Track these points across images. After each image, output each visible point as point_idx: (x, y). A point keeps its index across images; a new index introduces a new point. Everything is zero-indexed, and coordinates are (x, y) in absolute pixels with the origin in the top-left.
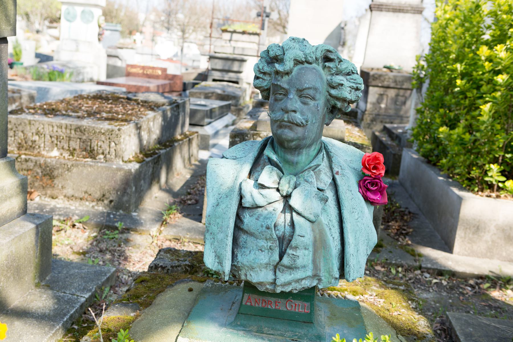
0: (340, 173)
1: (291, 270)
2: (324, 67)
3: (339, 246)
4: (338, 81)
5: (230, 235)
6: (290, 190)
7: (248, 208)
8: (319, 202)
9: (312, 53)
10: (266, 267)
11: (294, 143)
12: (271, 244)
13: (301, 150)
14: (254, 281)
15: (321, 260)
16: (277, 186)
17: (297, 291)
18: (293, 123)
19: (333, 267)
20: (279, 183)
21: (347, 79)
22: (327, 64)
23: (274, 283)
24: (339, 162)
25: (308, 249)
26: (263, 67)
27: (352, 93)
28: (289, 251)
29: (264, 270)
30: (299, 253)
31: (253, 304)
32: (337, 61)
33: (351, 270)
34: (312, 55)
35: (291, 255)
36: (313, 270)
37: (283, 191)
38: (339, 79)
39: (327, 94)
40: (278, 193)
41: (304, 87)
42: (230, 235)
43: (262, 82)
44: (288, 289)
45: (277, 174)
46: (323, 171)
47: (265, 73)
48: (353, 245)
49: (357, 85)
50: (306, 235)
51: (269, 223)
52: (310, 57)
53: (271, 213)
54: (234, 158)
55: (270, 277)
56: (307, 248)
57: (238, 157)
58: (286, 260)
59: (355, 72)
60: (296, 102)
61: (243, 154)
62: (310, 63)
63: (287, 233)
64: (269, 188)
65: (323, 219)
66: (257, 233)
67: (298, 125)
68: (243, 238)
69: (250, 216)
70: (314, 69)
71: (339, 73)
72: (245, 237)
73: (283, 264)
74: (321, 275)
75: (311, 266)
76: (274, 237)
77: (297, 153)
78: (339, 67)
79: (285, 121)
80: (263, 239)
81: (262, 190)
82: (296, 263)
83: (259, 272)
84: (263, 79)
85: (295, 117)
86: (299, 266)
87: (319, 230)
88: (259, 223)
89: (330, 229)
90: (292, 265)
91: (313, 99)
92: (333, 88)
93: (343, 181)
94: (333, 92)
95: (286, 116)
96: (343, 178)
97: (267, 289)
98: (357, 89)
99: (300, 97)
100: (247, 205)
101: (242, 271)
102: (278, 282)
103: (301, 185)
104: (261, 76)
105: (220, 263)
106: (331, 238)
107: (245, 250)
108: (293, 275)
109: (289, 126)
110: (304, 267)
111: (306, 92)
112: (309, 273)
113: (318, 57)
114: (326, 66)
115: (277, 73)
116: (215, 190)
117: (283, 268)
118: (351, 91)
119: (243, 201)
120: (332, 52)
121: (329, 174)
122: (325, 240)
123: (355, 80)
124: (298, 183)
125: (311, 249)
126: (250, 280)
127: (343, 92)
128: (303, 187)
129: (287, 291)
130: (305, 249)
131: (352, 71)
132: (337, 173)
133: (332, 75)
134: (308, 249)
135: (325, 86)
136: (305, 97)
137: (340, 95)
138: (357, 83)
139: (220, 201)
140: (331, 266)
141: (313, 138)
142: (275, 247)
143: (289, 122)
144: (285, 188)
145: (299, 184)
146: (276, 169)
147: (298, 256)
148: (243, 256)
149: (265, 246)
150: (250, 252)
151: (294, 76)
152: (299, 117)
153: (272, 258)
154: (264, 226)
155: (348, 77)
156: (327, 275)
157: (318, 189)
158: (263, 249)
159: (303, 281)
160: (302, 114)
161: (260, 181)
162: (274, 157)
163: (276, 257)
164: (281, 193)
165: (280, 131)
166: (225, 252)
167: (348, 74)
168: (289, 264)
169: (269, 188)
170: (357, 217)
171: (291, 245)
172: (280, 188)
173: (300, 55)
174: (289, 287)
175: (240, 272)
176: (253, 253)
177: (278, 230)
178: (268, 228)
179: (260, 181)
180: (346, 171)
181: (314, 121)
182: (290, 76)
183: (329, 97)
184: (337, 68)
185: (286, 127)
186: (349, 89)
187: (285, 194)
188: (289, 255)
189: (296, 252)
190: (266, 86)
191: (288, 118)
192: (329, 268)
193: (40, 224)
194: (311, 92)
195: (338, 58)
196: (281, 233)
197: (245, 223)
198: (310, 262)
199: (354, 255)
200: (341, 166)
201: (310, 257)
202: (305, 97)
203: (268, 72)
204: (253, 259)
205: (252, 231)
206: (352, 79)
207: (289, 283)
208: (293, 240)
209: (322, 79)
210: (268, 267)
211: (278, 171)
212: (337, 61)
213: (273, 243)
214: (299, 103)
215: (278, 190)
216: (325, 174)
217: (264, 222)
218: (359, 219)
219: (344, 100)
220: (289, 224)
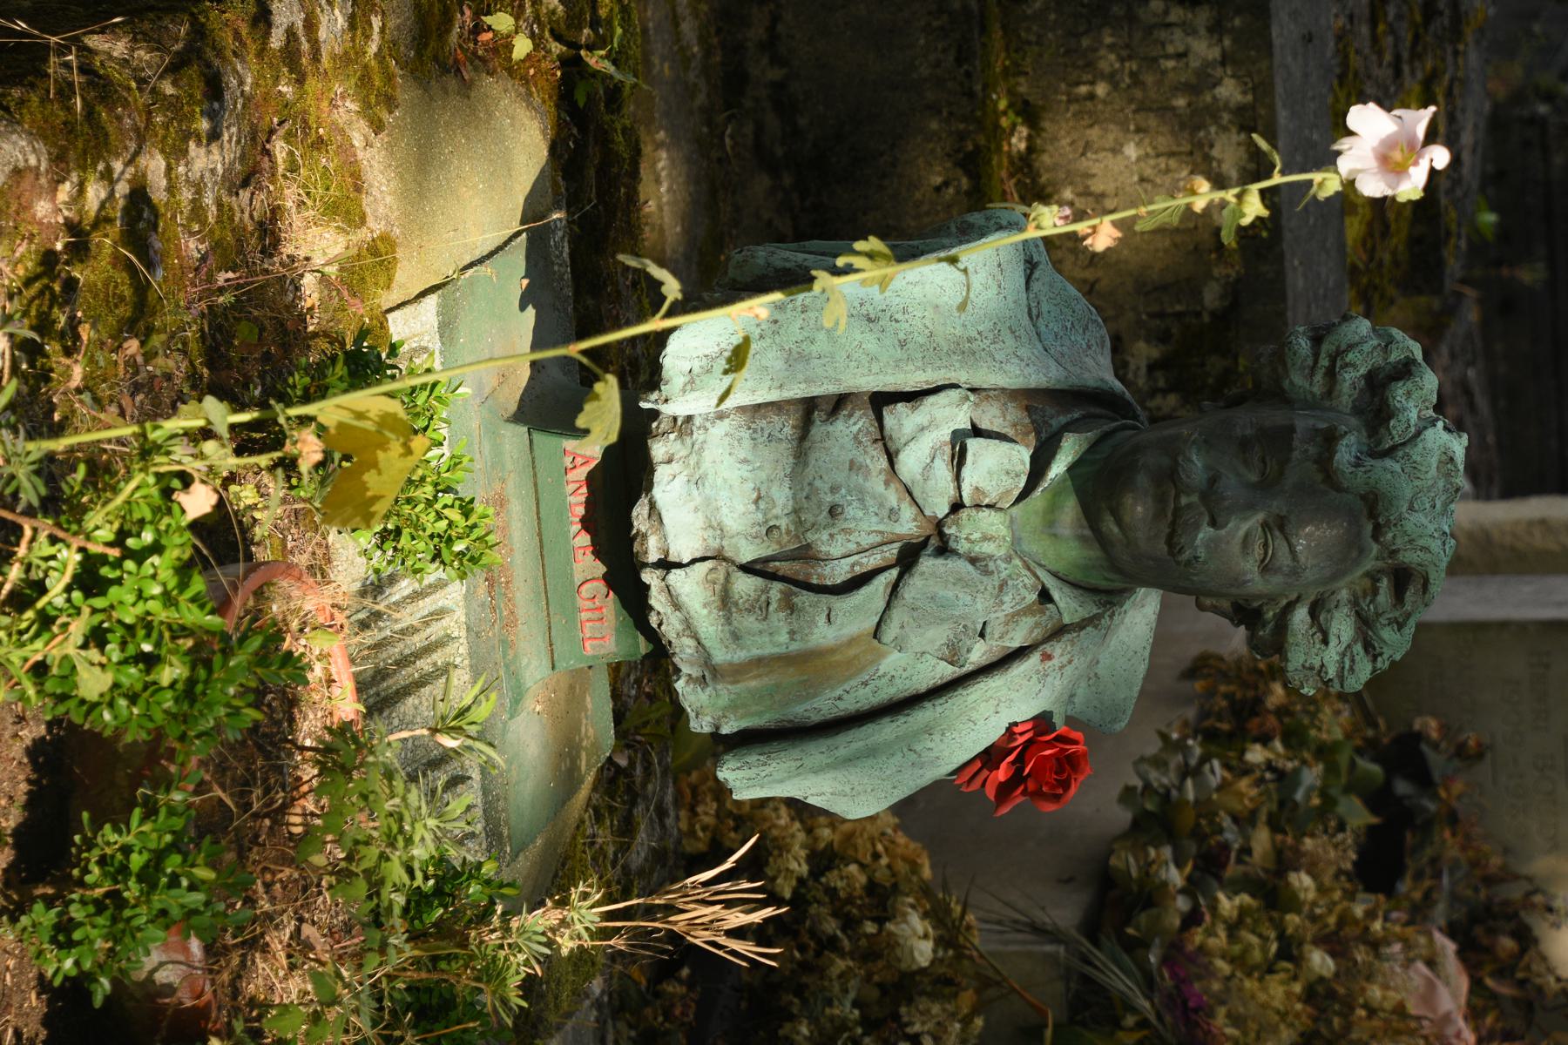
0: (1049, 664)
1: (719, 603)
2: (1373, 577)
3: (816, 718)
4: (1334, 630)
6: (963, 547)
7: (880, 419)
8: (944, 640)
9: (1406, 538)
10: (711, 527)
11: (1116, 530)
12: (783, 528)
14: (657, 492)
15: (766, 680)
16: (967, 500)
17: (655, 626)
18: (1173, 524)
20: (978, 506)
21: (1349, 646)
22: (1384, 584)
23: (666, 565)
25: (792, 639)
26: (1354, 365)
28: (776, 589)
29: (699, 520)
30: (778, 619)
31: (571, 476)
32: (1397, 614)
33: (754, 770)
35: (764, 598)
36: (731, 664)
38: (1343, 627)
39: (1294, 596)
40: (947, 511)
41: (1294, 541)
43: (1302, 368)
44: (657, 600)
45: (1008, 492)
47: (1331, 374)
50: (834, 627)
51: (852, 511)
52: (1394, 537)
53: (881, 505)
54: (1035, 312)
55: (682, 549)
56: (797, 637)
57: (1041, 323)
61: (1051, 337)
63: (828, 569)
64: (958, 478)
66: (810, 471)
69: (856, 437)
71: (1365, 624)
72: (788, 430)
73: (733, 579)
77: (1087, 532)
78: (1383, 621)
79: (1177, 497)
80: (794, 498)
81: (947, 457)
83: (692, 505)
84: (1313, 368)
88: (840, 477)
89: (865, 684)
90: (736, 604)
92: (1313, 613)
93: (1025, 682)
94: (1301, 616)
95: (1195, 498)
97: (645, 536)
100: (889, 420)
101: (678, 445)
102: (675, 576)
103: (985, 579)
104: (1324, 362)
105: (692, 382)
107: (747, 443)
108: (705, 612)
113: (1400, 556)
114: (1378, 581)
115: (1330, 439)
116: (917, 291)
119: (900, 407)
123: (1352, 669)
124: (991, 566)
125: (794, 647)
126: (658, 477)
129: (652, 602)
130: (792, 633)
131: (1381, 654)
134: (792, 639)
136: (1266, 545)
137: (1291, 640)
139: (884, 322)
142: (779, 543)
143: (1177, 511)
144: (966, 533)
146: (1022, 485)
147: (765, 619)
149: (775, 511)
150: (745, 461)
154: (837, 498)
155: (1358, 648)
158: (762, 505)
161: (973, 444)
162: (1058, 468)
163: (747, 553)
164: (949, 520)
165: (1142, 480)
167: (1368, 646)
168: (737, 597)
169: (958, 478)
171: (796, 594)
172: (964, 514)
175: (672, 436)
176: (746, 474)
178: (834, 511)
179: (973, 444)
182: (1322, 486)
183: (1284, 602)
184: (1378, 615)
185: (1161, 500)
186: (1317, 664)
187: (947, 531)
188: (765, 591)
190: (1292, 383)
191: (1189, 506)
195: (1408, 616)
196: (823, 549)
197: (831, 428)
198: (756, 652)
203: (1338, 387)
205: (812, 457)
206: (1353, 661)
208: (812, 597)
209: (1335, 576)
210: (710, 532)
211: (1016, 493)
212: (1397, 614)
213: (788, 532)
214: (1245, 527)
215: (957, 506)
217: (849, 492)
218: (913, 756)
220: (857, 569)
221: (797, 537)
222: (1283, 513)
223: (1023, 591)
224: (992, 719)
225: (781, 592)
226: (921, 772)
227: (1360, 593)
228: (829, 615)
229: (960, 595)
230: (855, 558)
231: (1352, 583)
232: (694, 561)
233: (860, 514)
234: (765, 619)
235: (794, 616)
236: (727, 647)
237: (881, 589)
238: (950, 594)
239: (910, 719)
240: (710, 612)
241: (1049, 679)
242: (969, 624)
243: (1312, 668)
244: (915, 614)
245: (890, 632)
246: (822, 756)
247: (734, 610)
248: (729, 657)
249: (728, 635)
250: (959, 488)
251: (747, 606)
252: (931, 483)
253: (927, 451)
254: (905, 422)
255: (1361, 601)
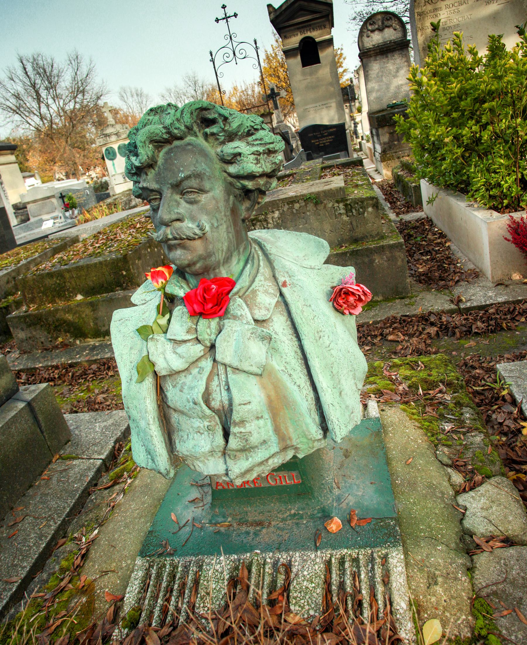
0: (288, 283)
2: (206, 136)
3: (312, 395)
4: (232, 151)
5: (151, 422)
6: (213, 337)
12: (208, 424)
13: (217, 271)
16: (194, 336)
19: (308, 428)
20: (196, 330)
22: (208, 130)
24: (284, 267)
25: (262, 417)
27: (262, 161)
28: (234, 430)
29: (212, 459)
30: (250, 427)
32: (220, 121)
33: (335, 426)
34: (177, 125)
35: (238, 435)
36: (279, 443)
37: (204, 341)
39: (225, 175)
42: (151, 422)
46: (261, 289)
48: (329, 390)
49: (268, 146)
52: (176, 129)
56: (260, 416)
57: (147, 300)
58: (233, 443)
59: (259, 127)
60: (178, 204)
62: (181, 138)
64: (185, 341)
65: (276, 365)
67: (189, 239)
68: (175, 417)
70: (189, 144)
71: (231, 137)
74: (295, 444)
75: (274, 439)
76: (207, 414)
79: (169, 240)
82: (249, 442)
85: (181, 228)
86: (256, 444)
87: (273, 384)
89: (290, 375)
90: (244, 446)
91: (202, 191)
92: (230, 162)
93: (296, 294)
94: (232, 169)
96: (295, 289)
98: (270, 152)
99: (182, 194)
103: (226, 327)
106: (296, 388)
108: (250, 459)
109: (179, 245)
110: (265, 442)
111: (186, 184)
112: (274, 448)
113: (188, 124)
114: (206, 133)
117: (235, 453)
118: (257, 159)
120: (209, 109)
121: (272, 290)
122: (284, 397)
123: (261, 139)
125: (266, 416)
127: (245, 165)
128: (229, 329)
130: (258, 418)
131: (252, 127)
132: (284, 284)
133: (223, 143)
135: (218, 165)
136: (188, 192)
138: (266, 144)
140: (305, 428)
141: (225, 248)
142: (215, 426)
143: (175, 239)
145: (223, 326)
147: (250, 432)
148: (181, 443)
150: (188, 435)
151: (162, 167)
152: (190, 225)
153: (214, 443)
155: (250, 139)
156: (305, 440)
157: (256, 321)
159: (270, 461)
160: (193, 219)
163: (220, 440)
166: (153, 447)
167: (249, 134)
168: (240, 447)
169: (185, 341)
170: (328, 343)
171: (234, 421)
172: (199, 338)
173: (157, 131)
174: (252, 474)
176: (192, 437)
177: (213, 399)
180: (296, 278)
181: (216, 225)
182: (157, 169)
183: (229, 178)
184: (223, 130)
186: (253, 157)
188: (235, 434)
189: (245, 428)
191: (172, 233)
192: (303, 432)
193: (33, 399)
194: (194, 183)
195: (220, 115)
196: (218, 403)
198: (271, 433)
199: (334, 404)
200: (287, 272)
201: (269, 426)
202: (188, 192)
204: (193, 448)
206: (256, 140)
207: (249, 471)
212: (220, 121)
213: (210, 422)
214: (183, 203)
215: (198, 341)
216: (266, 292)
219: (251, 177)
221: (211, 418)
222: (169, 186)
223: (235, 306)
224: (313, 308)
225: (235, 427)
226: (340, 340)
227: (218, 142)
228: (244, 404)
229: (235, 338)
230: (222, 388)
231: (213, 146)
232: (226, 463)
233: (196, 390)
234: (250, 432)
235: (247, 420)
236: (270, 446)
237: (234, 376)
238: (234, 343)
239: (308, 352)
240: (251, 456)
241: (294, 281)
242: (251, 331)
243: (257, 159)
244: (244, 360)
245: (255, 369)
246: (327, 394)
247: (248, 446)
248: (275, 445)
249: (264, 446)
250: (189, 341)
251: (244, 441)
252: (184, 355)
253: (174, 356)
254: (162, 367)
255: (220, 140)
